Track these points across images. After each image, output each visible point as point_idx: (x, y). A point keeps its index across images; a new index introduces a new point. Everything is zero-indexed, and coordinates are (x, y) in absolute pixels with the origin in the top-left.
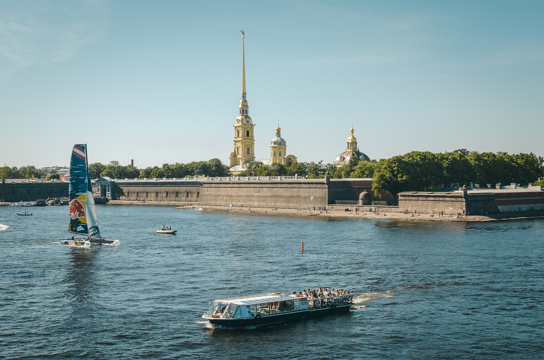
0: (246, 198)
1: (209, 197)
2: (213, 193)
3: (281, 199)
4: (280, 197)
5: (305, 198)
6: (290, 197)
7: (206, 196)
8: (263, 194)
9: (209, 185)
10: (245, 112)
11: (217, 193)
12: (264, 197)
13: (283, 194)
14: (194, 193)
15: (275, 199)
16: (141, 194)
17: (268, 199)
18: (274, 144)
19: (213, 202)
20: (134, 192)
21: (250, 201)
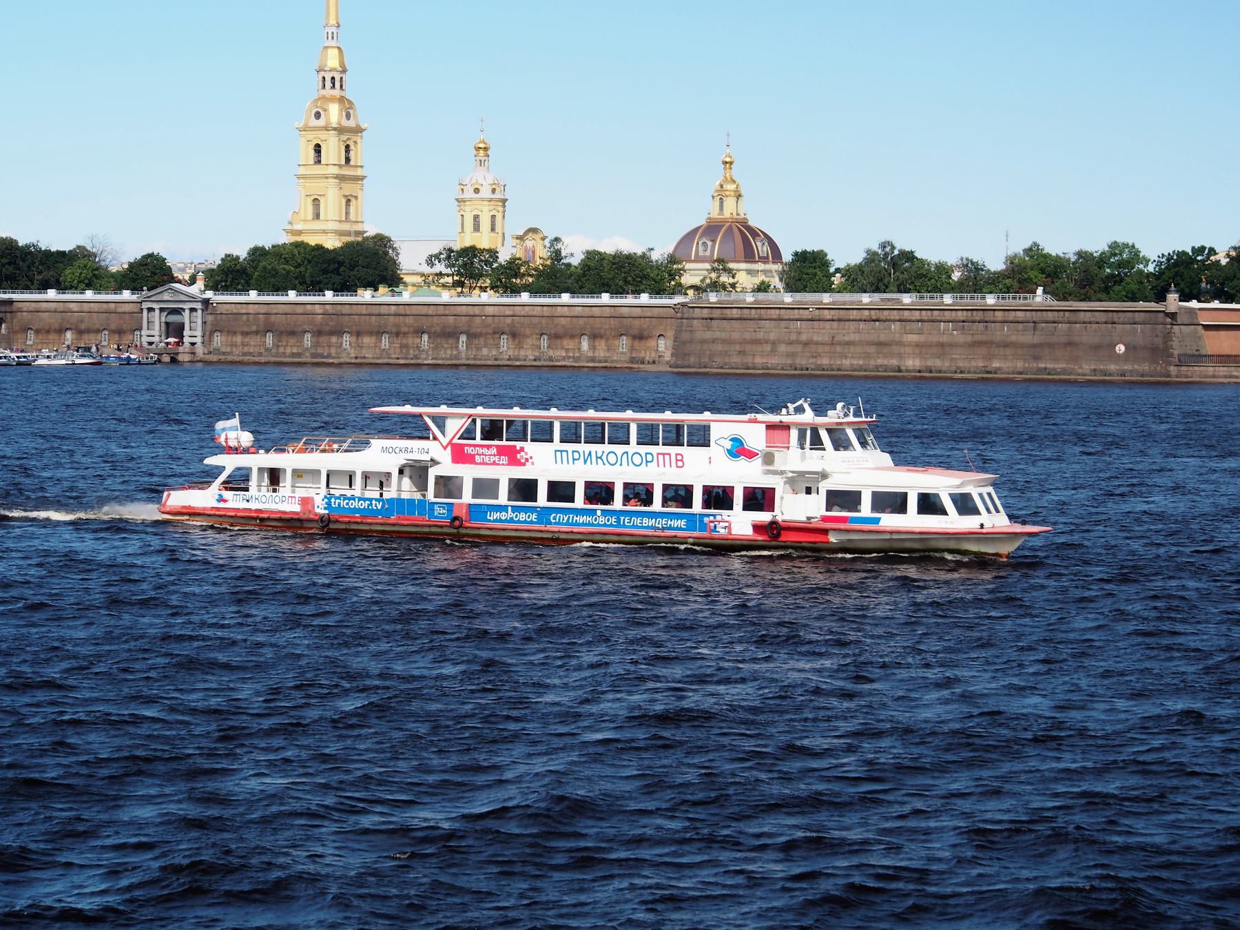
0: (872, 349)
1: (719, 347)
2: (736, 336)
3: (1008, 351)
4: (1006, 345)
5: (1096, 348)
6: (1040, 345)
7: (703, 342)
8: (934, 339)
9: (717, 313)
10: (337, 85)
11: (747, 336)
12: (942, 345)
13: (1014, 338)
14: (526, 336)
15: (983, 351)
16: (323, 339)
17: (959, 350)
18: (477, 191)
19: (736, 360)
20: (292, 333)
21: (892, 355)
